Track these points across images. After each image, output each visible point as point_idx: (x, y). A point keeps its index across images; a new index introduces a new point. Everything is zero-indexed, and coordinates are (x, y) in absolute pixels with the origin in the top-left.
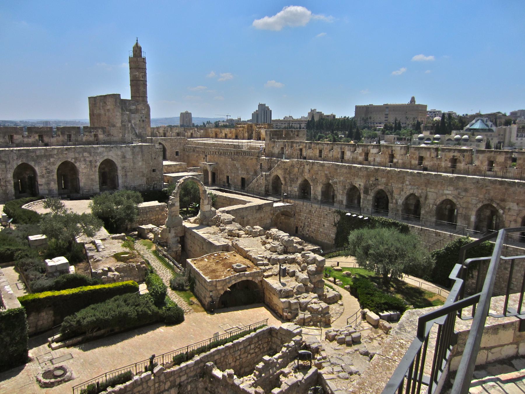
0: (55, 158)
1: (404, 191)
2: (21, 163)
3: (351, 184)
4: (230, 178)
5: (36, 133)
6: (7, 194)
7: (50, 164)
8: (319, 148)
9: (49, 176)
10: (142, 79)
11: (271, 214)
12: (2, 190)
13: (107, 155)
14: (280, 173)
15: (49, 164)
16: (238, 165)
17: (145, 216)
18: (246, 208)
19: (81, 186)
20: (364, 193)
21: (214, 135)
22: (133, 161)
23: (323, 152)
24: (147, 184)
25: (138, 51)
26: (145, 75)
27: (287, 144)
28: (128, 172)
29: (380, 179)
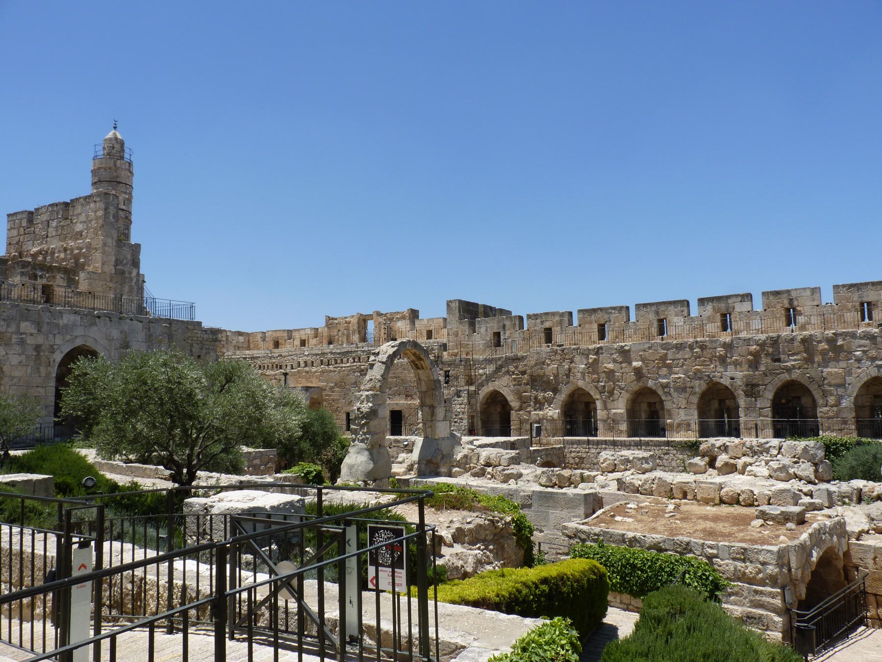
10: (124, 207)
13: (84, 336)
25: (117, 147)
26: (129, 201)
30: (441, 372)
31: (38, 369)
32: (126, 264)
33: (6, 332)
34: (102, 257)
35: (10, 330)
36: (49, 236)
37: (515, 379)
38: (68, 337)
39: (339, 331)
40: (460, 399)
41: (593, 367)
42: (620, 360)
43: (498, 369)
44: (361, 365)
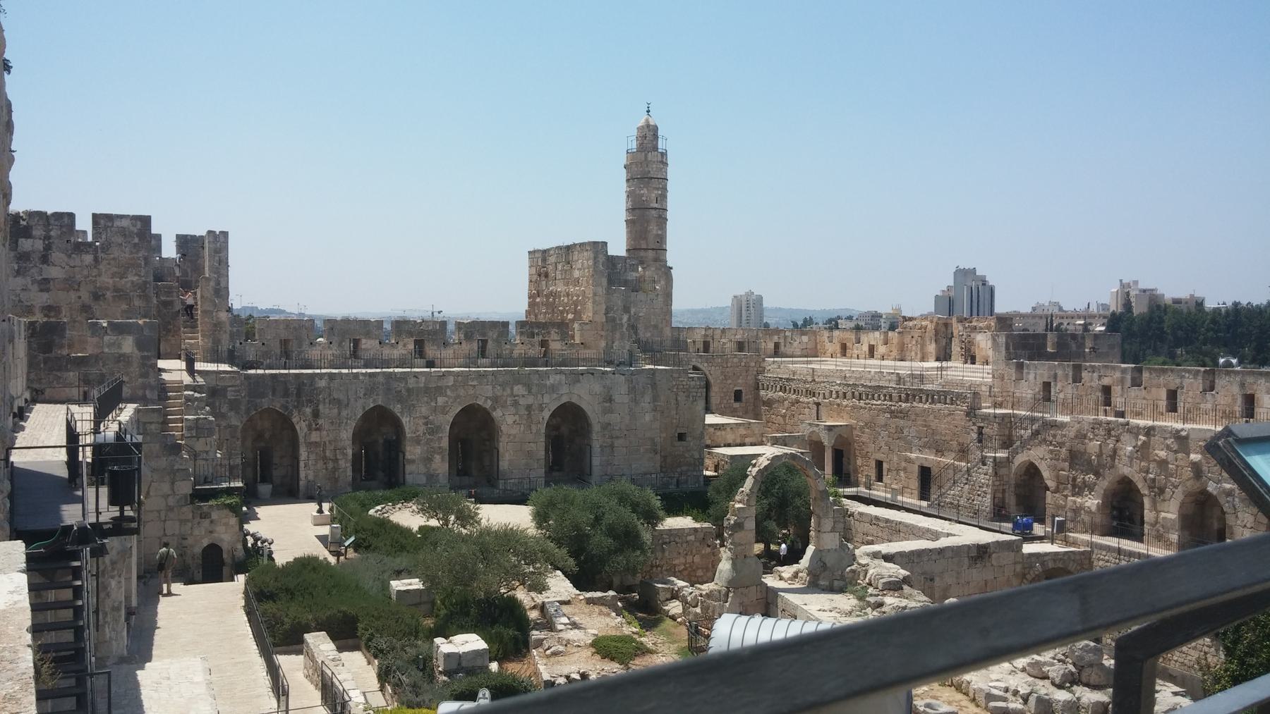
0: (446, 396)
2: (372, 405)
4: (885, 466)
5: (410, 334)
6: (336, 480)
7: (435, 411)
10: (656, 206)
11: (1016, 575)
12: (327, 469)
14: (1038, 455)
15: (435, 410)
16: (911, 432)
17: (659, 554)
19: (501, 468)
21: (838, 348)
24: (661, 472)
25: (650, 137)
26: (663, 197)
27: (1060, 373)
28: (617, 437)
30: (973, 427)
32: (617, 310)
33: (502, 395)
34: (593, 307)
35: (505, 394)
36: (557, 278)
37: (1051, 452)
38: (555, 396)
39: (912, 337)
40: (985, 467)
41: (1143, 451)
42: (1175, 447)
43: (1036, 434)
44: (891, 405)
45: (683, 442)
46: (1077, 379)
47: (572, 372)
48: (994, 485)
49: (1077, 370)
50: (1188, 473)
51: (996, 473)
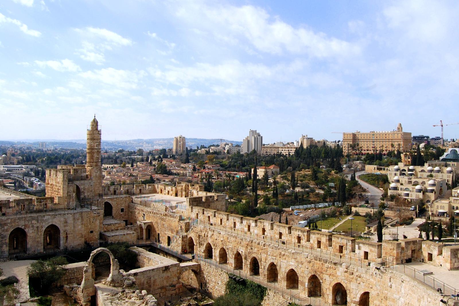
0: (8, 226)
1: (268, 260)
3: (237, 252)
4: (160, 235)
8: (220, 218)
9: (2, 240)
15: (3, 231)
16: (166, 225)
18: (153, 270)
19: (28, 247)
20: (245, 259)
22: (74, 225)
23: (223, 221)
27: (200, 211)
28: (69, 234)
29: (253, 248)
31: (38, 233)
35: (29, 223)
38: (47, 223)
45: (92, 234)
46: (203, 213)
47: (53, 215)
48: (182, 244)
49: (203, 210)
50: (221, 243)
51: (183, 240)
